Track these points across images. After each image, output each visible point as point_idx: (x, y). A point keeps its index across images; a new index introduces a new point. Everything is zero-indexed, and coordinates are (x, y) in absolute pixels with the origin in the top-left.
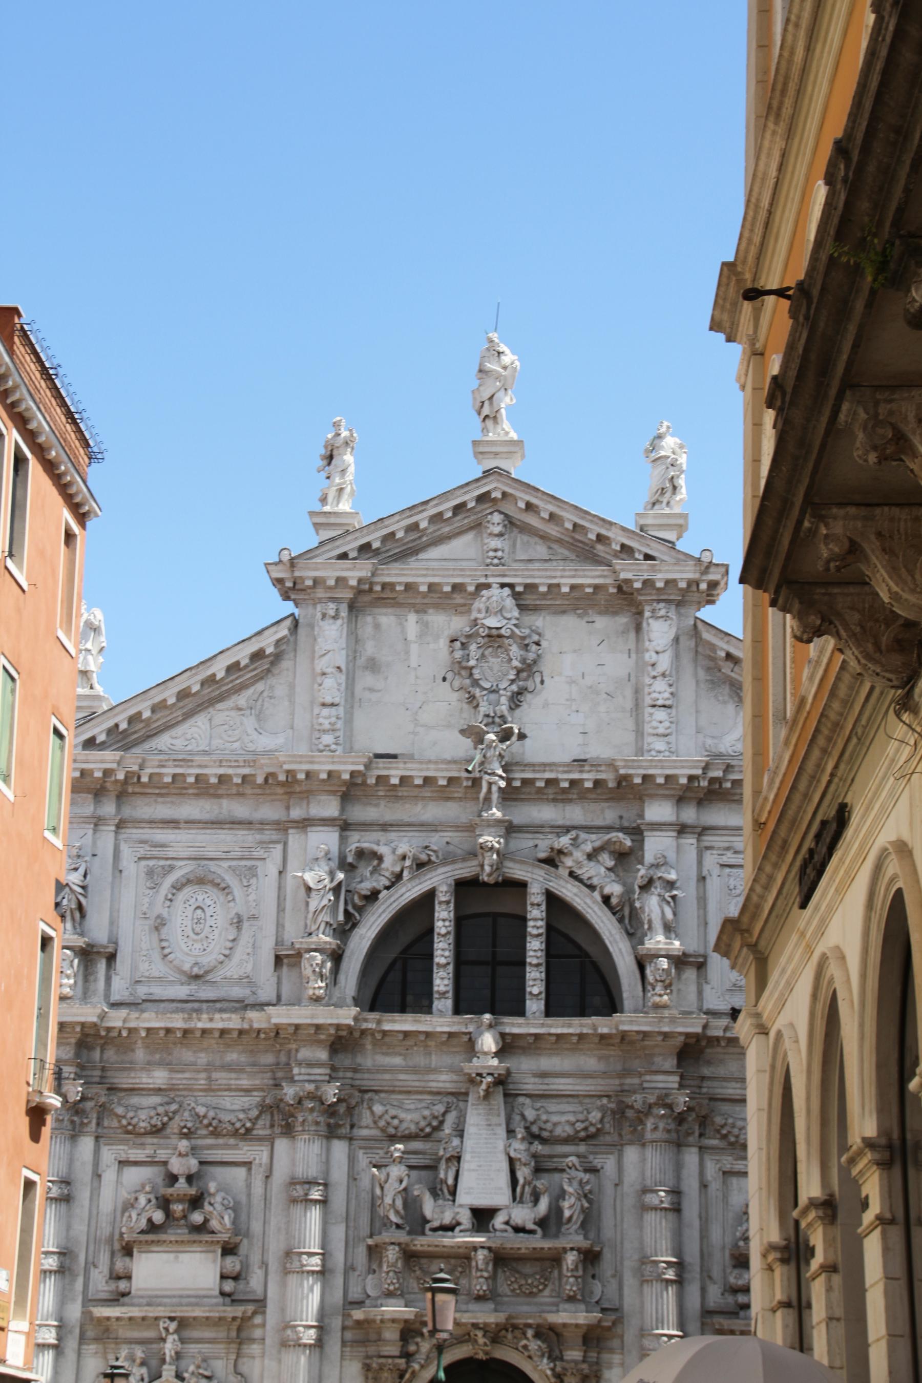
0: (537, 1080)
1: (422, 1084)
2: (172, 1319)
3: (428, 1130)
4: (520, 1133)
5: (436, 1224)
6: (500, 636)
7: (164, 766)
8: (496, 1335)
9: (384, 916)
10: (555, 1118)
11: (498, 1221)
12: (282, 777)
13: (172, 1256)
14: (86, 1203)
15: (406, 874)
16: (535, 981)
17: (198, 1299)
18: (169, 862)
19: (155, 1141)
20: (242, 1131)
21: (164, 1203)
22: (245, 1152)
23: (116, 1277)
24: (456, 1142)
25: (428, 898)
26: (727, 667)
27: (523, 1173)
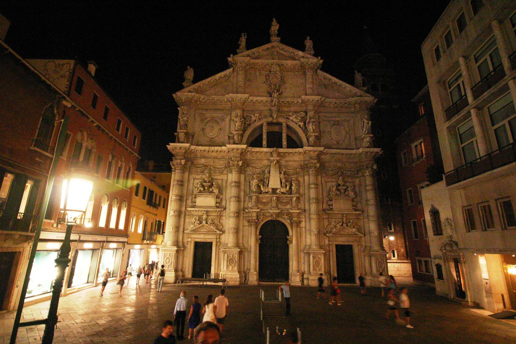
4: (282, 173)
8: (278, 215)
10: (289, 171)
11: (278, 191)
14: (186, 187)
16: (285, 143)
17: (211, 207)
21: (203, 186)
23: (192, 202)
24: (268, 175)
25: (262, 126)
27: (283, 181)
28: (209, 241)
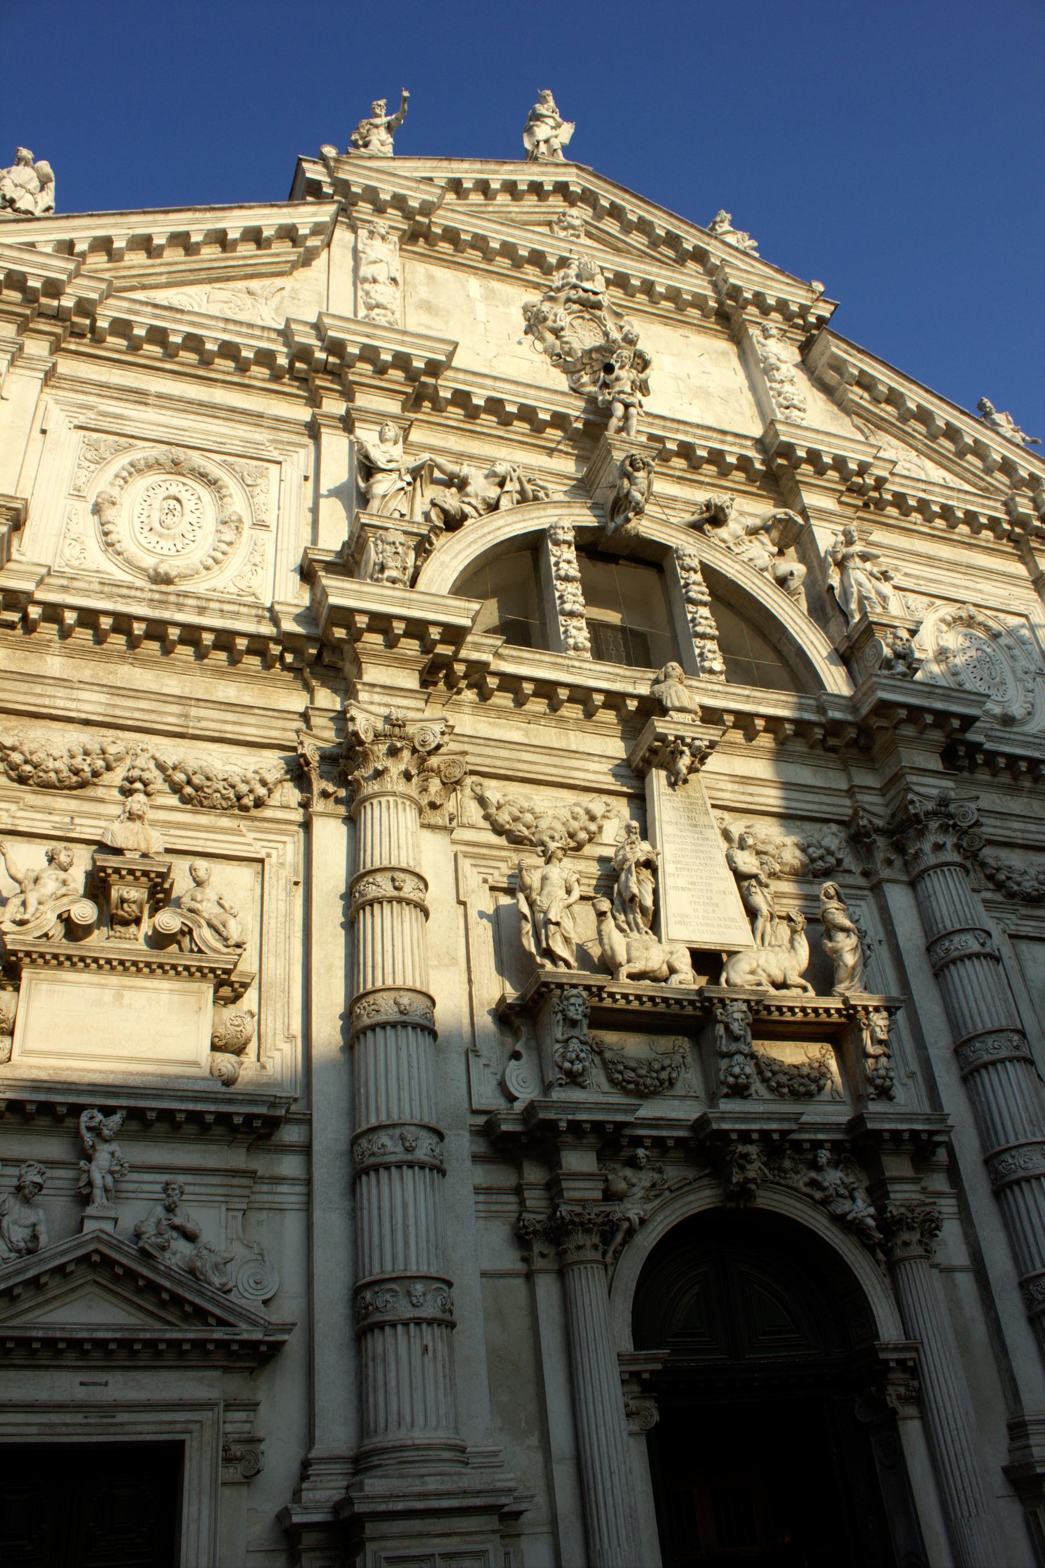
0: (736, 787)
1: (562, 772)
2: (108, 1111)
3: (583, 836)
5: (637, 967)
6: (598, 306)
7: (136, 313)
9: (474, 547)
12: (320, 355)
13: (108, 995)
15: (505, 503)
18: (123, 440)
19: (73, 805)
20: (248, 801)
22: (248, 839)
25: (534, 545)
26: (856, 393)
28: (144, 1428)
